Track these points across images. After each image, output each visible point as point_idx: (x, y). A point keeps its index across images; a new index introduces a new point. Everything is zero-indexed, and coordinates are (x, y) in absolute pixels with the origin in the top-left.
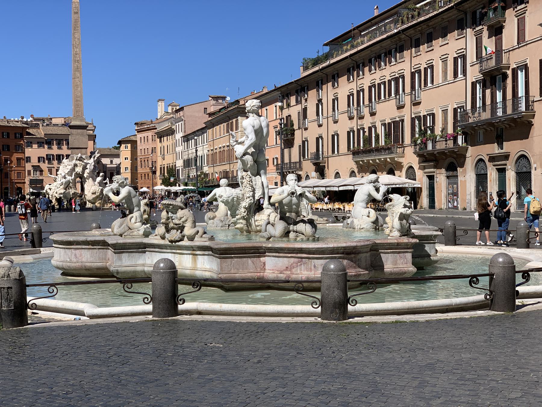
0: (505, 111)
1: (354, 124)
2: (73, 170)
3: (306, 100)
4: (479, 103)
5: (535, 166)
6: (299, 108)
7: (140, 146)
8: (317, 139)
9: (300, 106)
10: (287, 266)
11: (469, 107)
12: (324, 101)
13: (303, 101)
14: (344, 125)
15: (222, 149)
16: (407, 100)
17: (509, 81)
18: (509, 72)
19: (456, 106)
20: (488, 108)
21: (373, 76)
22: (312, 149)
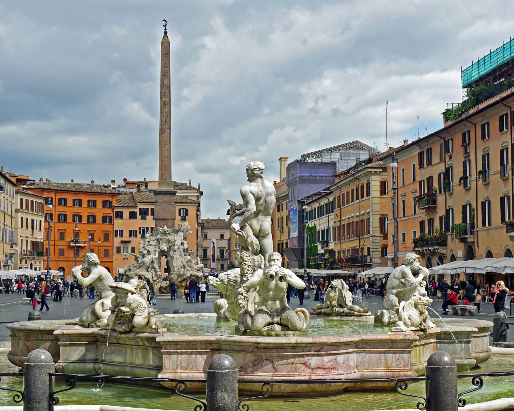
3: (450, 157)
6: (442, 168)
8: (464, 207)
9: (443, 165)
10: (241, 365)
12: (472, 157)
13: (447, 158)
15: (351, 220)
22: (458, 220)
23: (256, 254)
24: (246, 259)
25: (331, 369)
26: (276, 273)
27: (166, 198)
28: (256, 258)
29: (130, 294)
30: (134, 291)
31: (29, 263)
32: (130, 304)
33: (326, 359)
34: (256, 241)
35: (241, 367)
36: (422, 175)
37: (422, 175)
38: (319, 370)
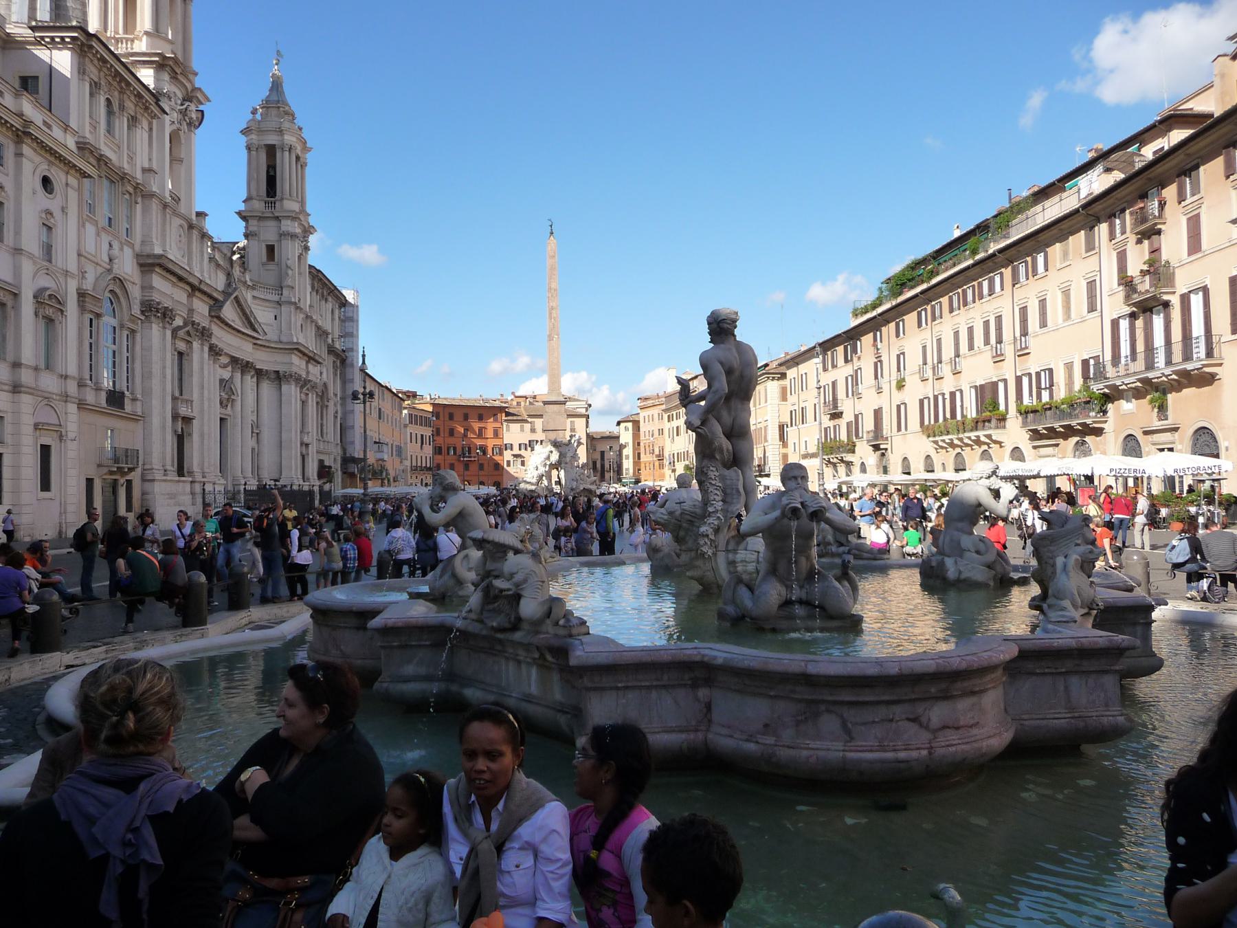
0: (1169, 362)
1: (928, 390)
2: (548, 458)
4: (1125, 349)
5: (1226, 444)
6: (848, 370)
7: (644, 428)
11: (1108, 356)
12: (885, 358)
13: (855, 359)
14: (915, 391)
16: (1008, 350)
17: (1176, 314)
18: (1175, 300)
19: (1086, 357)
20: (1141, 357)
21: (957, 319)
23: (727, 466)
24: (711, 474)
25: (971, 727)
26: (802, 503)
27: (556, 407)
28: (726, 472)
29: (511, 554)
30: (520, 546)
31: (420, 478)
32: (512, 575)
33: (963, 704)
34: (726, 444)
35: (766, 726)
36: (827, 379)
37: (827, 379)
38: (948, 732)
